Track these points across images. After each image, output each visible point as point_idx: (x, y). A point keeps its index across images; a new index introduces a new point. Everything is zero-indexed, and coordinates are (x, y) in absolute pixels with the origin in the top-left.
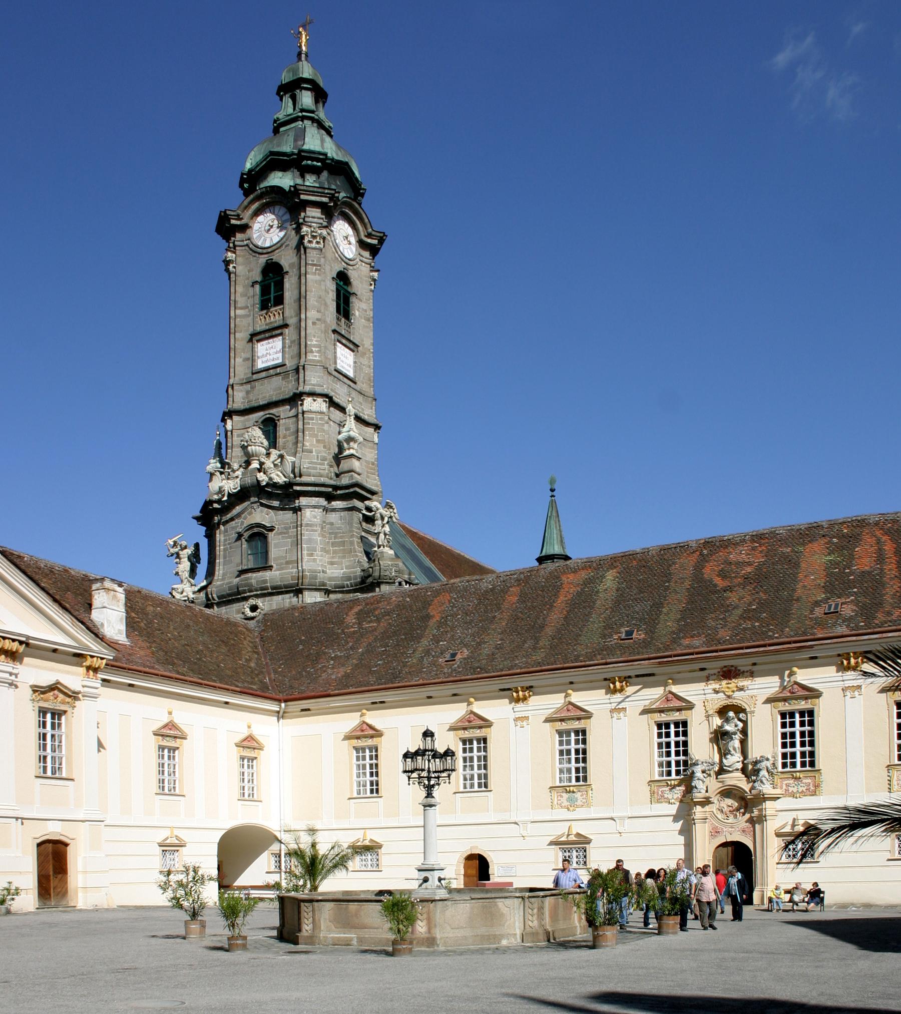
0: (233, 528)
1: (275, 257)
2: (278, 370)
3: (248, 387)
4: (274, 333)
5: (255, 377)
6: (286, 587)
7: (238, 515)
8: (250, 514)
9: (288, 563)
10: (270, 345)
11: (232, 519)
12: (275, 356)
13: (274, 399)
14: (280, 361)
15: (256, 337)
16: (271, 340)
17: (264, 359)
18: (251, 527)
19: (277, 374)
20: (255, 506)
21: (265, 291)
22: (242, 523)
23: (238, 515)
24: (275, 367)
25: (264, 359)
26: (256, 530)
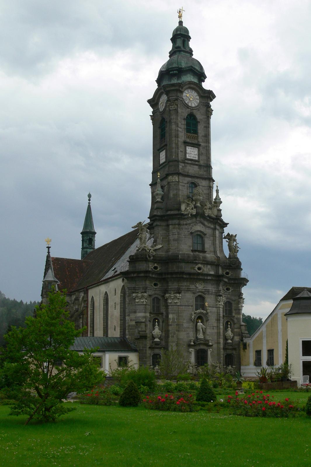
0: (186, 229)
1: (195, 112)
2: (197, 163)
3: (183, 165)
4: (195, 146)
5: (186, 161)
6: (212, 262)
7: (190, 224)
8: (195, 225)
9: (211, 251)
10: (192, 150)
11: (186, 224)
12: (195, 156)
13: (197, 175)
14: (197, 159)
15: (186, 144)
16: (192, 148)
17: (190, 155)
18: (198, 231)
19: (196, 165)
20: (198, 222)
21: (188, 124)
22: (191, 228)
23: (190, 224)
24: (195, 161)
25: (190, 155)
26: (199, 233)
